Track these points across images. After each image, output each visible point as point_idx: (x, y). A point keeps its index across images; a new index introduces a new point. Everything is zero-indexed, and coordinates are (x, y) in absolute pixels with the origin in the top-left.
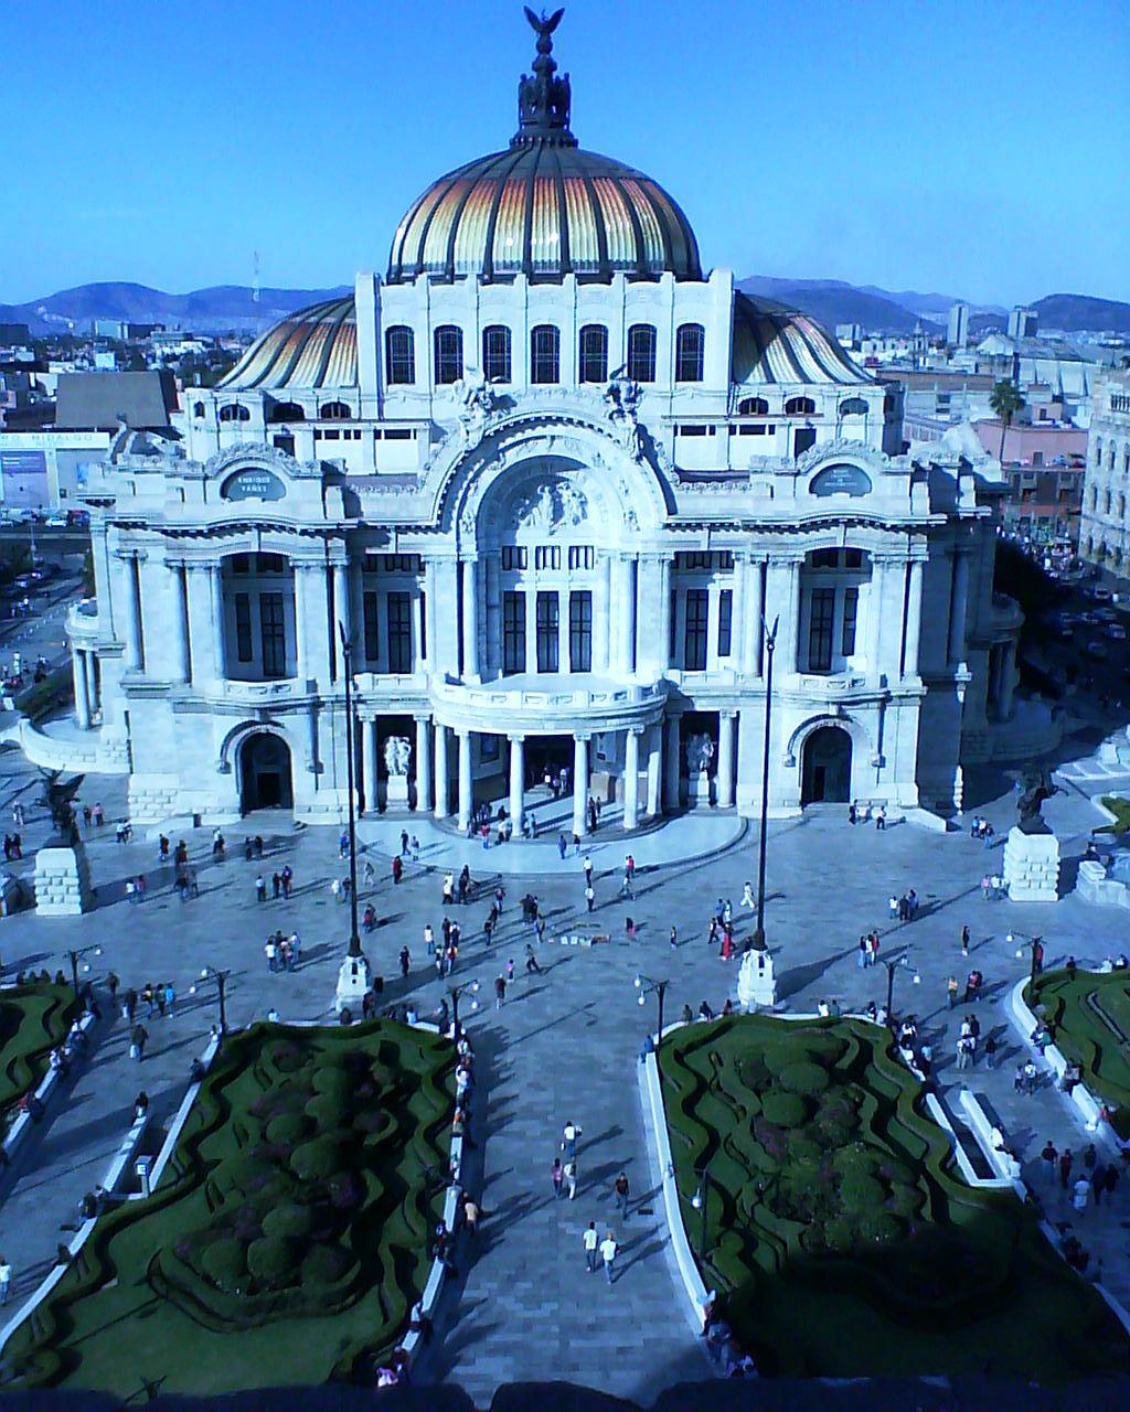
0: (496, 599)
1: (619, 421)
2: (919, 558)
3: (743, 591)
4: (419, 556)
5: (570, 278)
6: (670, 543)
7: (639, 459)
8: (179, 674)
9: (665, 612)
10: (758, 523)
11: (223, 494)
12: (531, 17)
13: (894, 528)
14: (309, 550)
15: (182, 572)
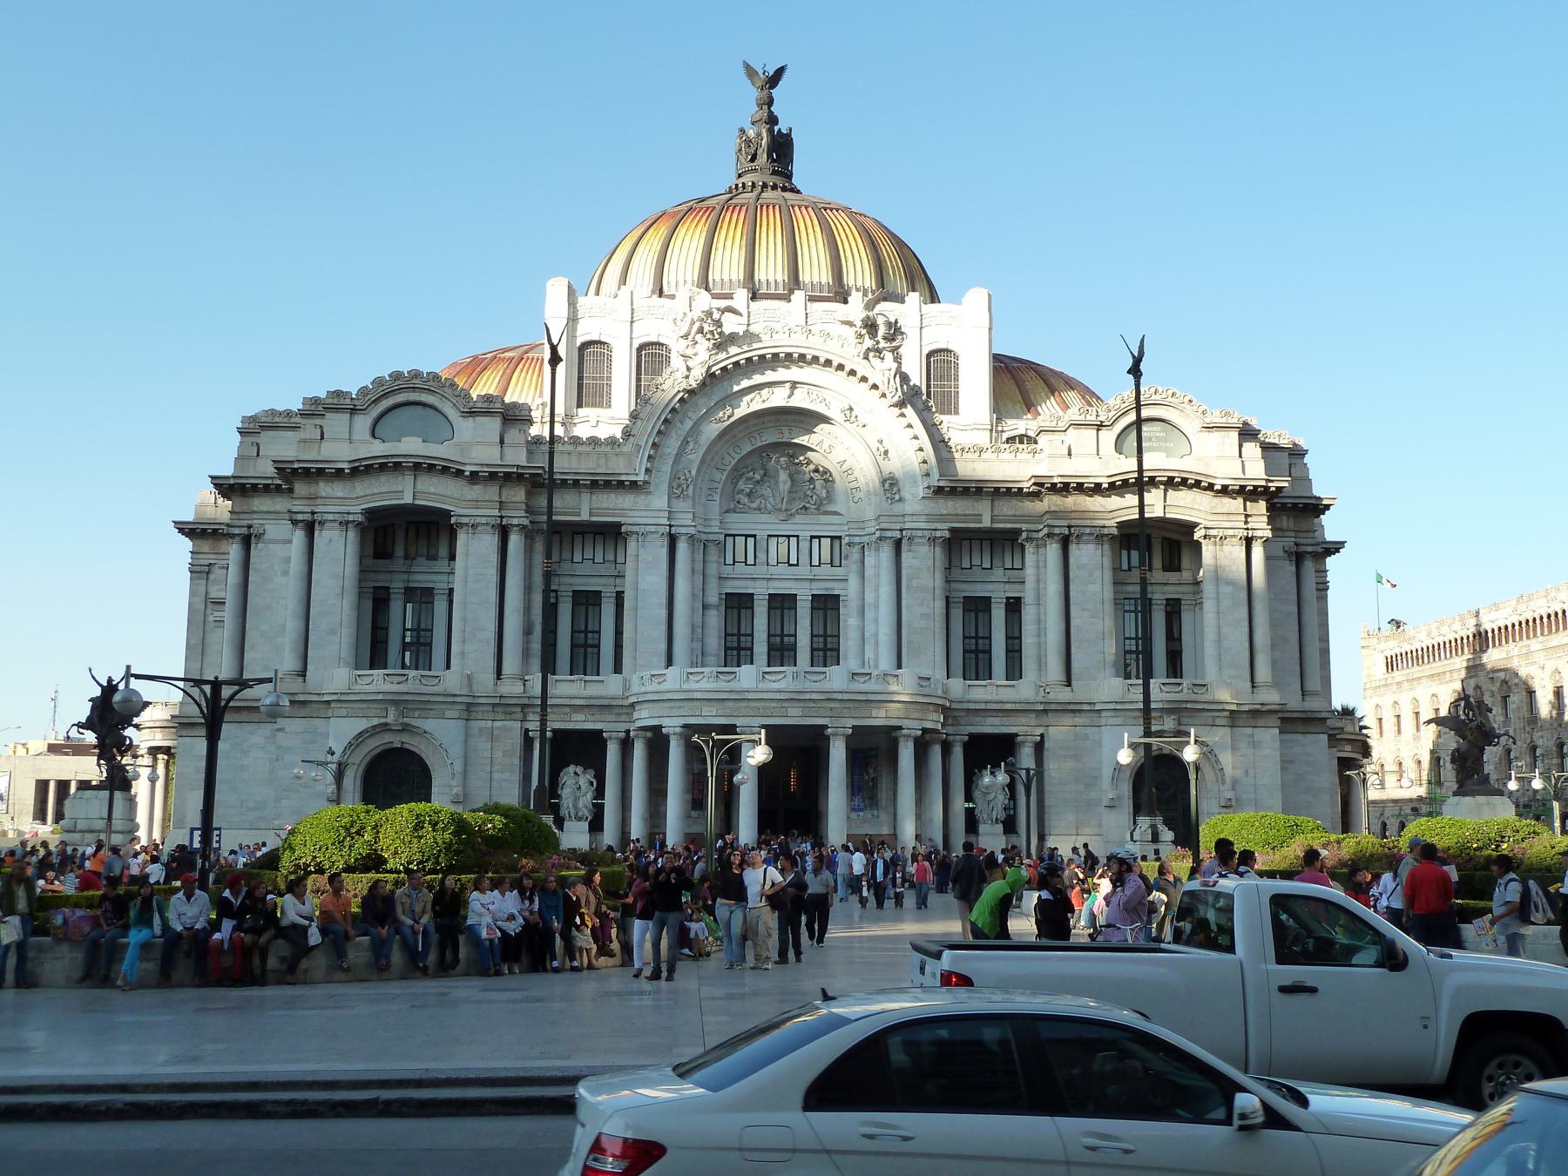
0: (713, 598)
1: (875, 361)
2: (1259, 533)
3: (1038, 581)
4: (619, 525)
5: (799, 296)
6: (941, 518)
7: (901, 404)
8: (289, 663)
9: (940, 605)
10: (1056, 480)
11: (373, 435)
12: (750, 71)
13: (1225, 491)
14: (476, 503)
15: (310, 528)
